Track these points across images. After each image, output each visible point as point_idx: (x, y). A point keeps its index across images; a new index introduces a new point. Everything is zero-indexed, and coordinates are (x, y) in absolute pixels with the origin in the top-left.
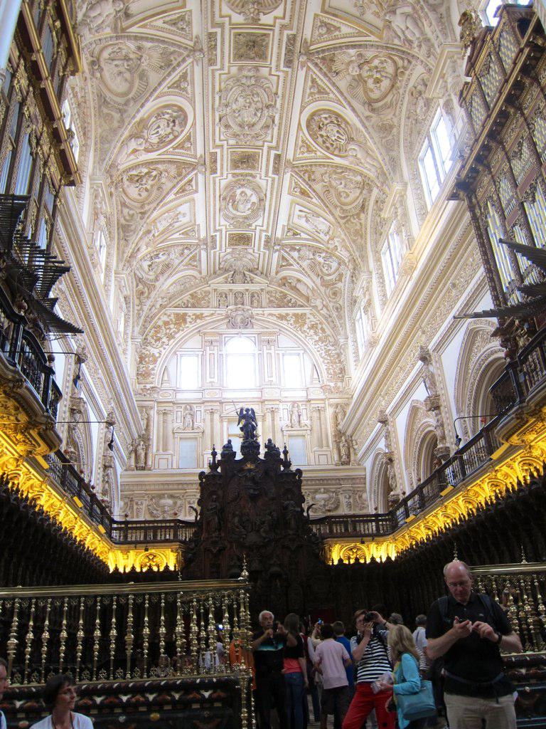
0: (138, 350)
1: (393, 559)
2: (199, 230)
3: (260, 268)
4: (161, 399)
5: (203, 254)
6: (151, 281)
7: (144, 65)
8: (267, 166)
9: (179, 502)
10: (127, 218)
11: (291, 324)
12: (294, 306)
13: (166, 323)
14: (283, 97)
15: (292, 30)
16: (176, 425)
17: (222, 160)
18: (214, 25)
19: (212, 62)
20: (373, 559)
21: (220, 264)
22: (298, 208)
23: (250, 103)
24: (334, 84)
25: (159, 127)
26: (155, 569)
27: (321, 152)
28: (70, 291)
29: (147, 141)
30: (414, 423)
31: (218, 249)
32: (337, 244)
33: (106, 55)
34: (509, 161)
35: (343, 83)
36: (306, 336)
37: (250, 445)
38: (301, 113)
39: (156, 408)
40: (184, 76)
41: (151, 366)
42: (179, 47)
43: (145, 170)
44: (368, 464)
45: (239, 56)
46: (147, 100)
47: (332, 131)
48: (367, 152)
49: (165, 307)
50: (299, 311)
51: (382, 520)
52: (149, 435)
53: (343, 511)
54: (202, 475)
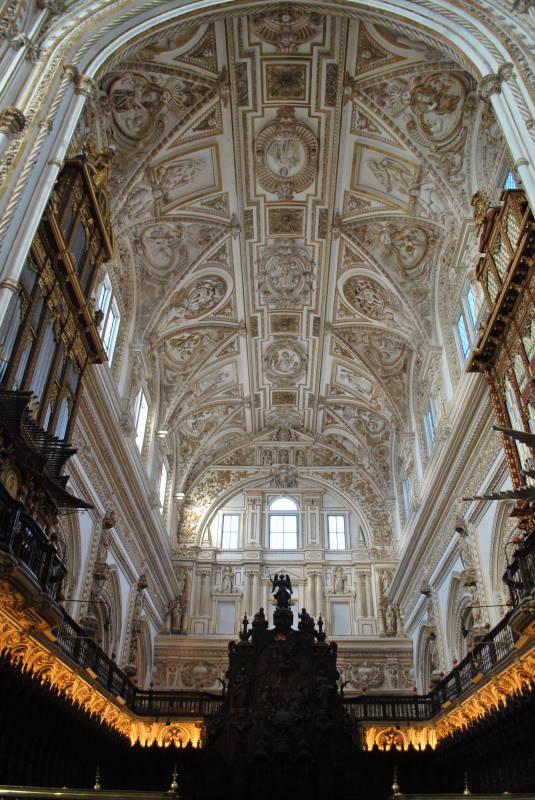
1: (434, 747)
2: (242, 389)
3: (306, 426)
4: (200, 558)
5: (248, 413)
6: (196, 439)
7: (184, 240)
8: (308, 328)
9: (214, 670)
10: (171, 379)
12: (341, 464)
13: (211, 481)
14: (319, 265)
15: (323, 204)
16: (215, 587)
17: (263, 323)
18: (250, 203)
19: (249, 236)
20: (411, 746)
21: (265, 422)
22: (340, 368)
23: (288, 271)
24: (367, 253)
25: (199, 295)
26: (178, 744)
27: (359, 315)
28: (99, 458)
29: (187, 309)
30: (455, 596)
31: (262, 407)
32: (380, 403)
33: (148, 234)
34: (521, 338)
35: (378, 253)
36: (352, 496)
37: (283, 615)
38: (338, 278)
39: (194, 569)
40: (223, 250)
41: (192, 526)
42: (217, 224)
43: (187, 335)
44: (415, 636)
45: (275, 230)
46: (187, 272)
47: (368, 295)
48: (403, 315)
49: (209, 464)
50: (346, 470)
51: (421, 703)
52: (186, 597)
53: (388, 688)
54: (232, 644)
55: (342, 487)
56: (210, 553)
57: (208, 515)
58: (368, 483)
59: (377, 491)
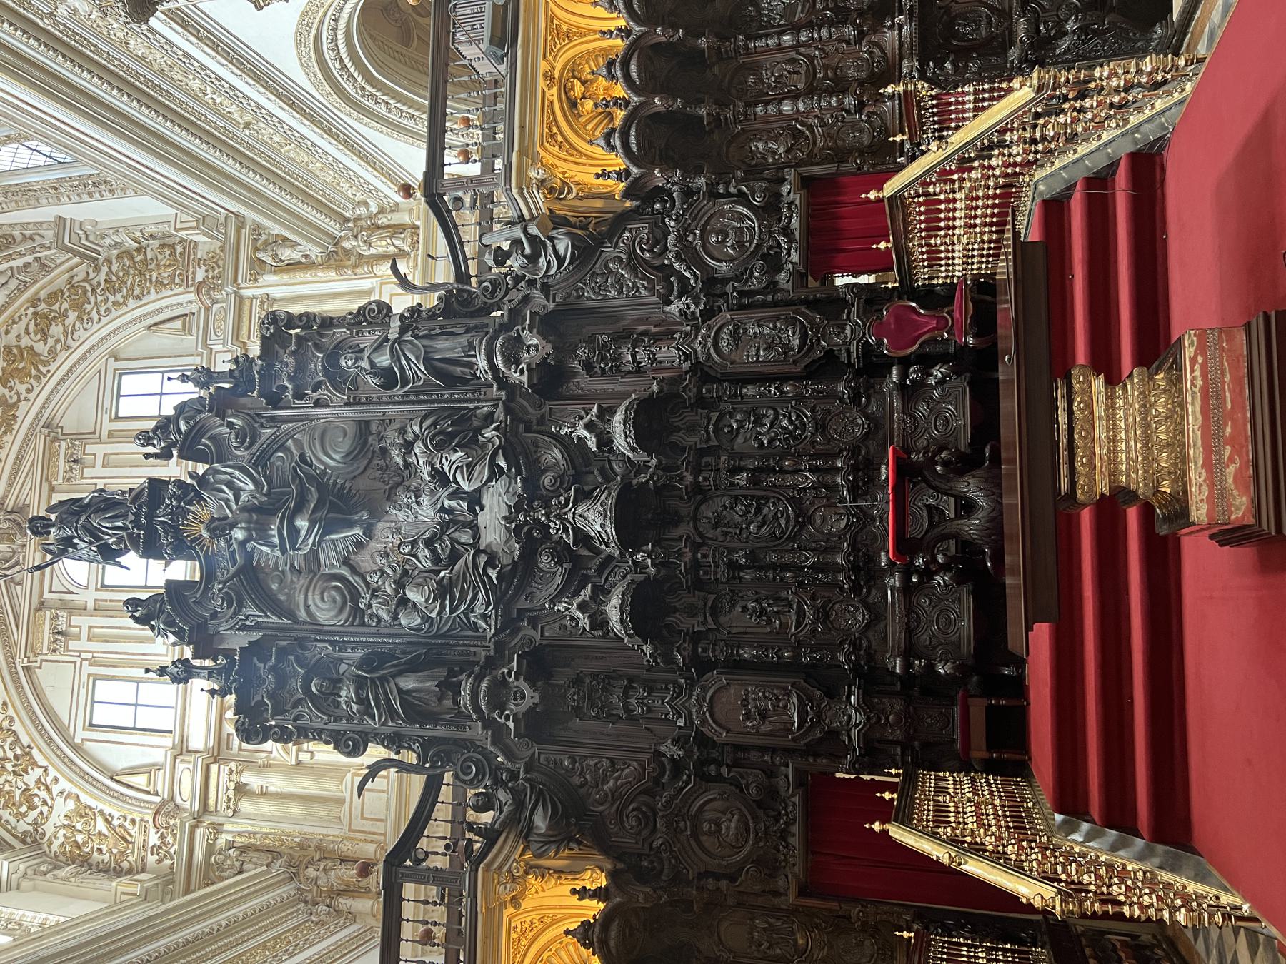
0: (43, 868)
11: (29, 391)
39: (221, 820)
41: (101, 825)
55: (38, 378)
56: (180, 767)
57: (83, 775)
58: (34, 301)
59: (57, 279)
